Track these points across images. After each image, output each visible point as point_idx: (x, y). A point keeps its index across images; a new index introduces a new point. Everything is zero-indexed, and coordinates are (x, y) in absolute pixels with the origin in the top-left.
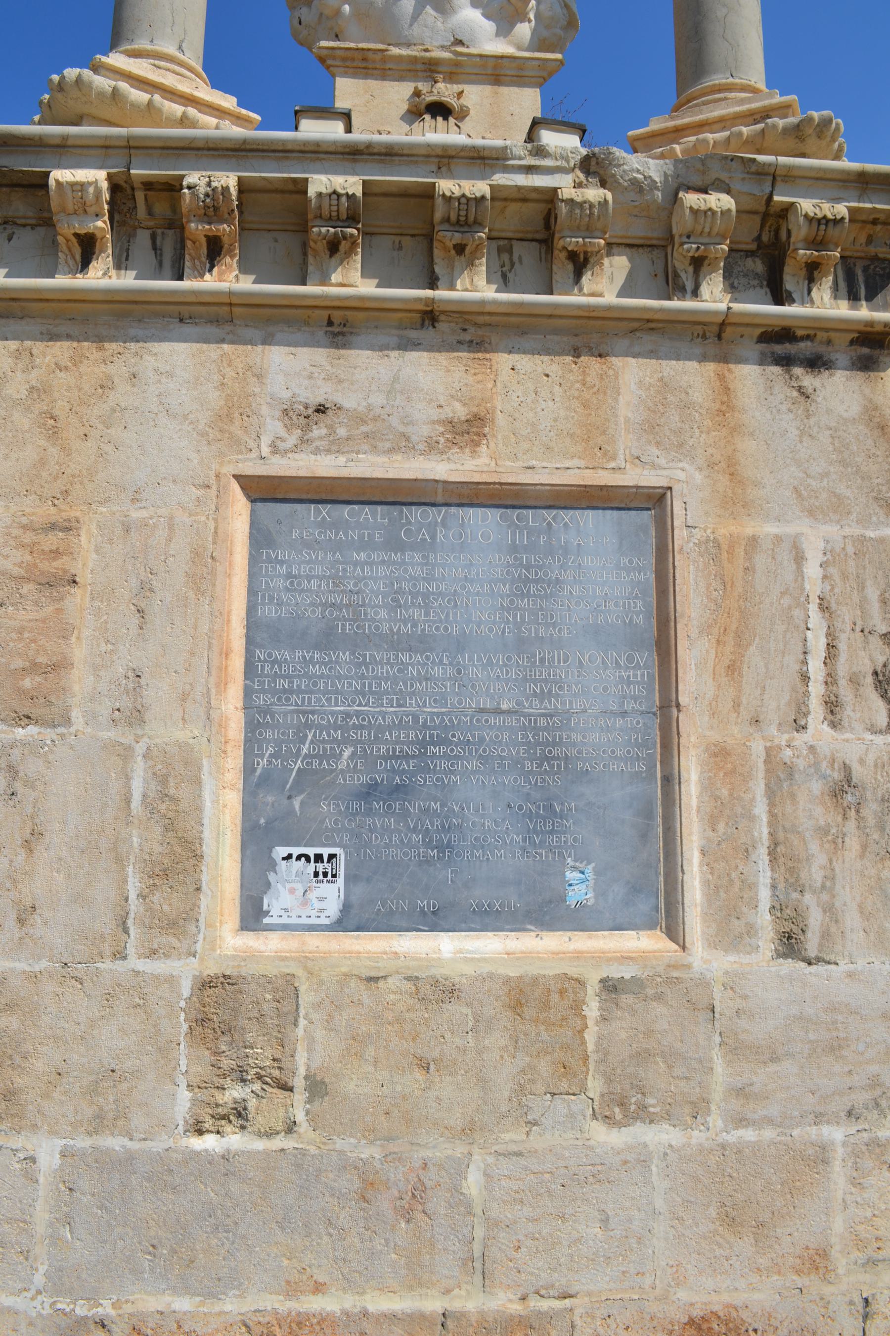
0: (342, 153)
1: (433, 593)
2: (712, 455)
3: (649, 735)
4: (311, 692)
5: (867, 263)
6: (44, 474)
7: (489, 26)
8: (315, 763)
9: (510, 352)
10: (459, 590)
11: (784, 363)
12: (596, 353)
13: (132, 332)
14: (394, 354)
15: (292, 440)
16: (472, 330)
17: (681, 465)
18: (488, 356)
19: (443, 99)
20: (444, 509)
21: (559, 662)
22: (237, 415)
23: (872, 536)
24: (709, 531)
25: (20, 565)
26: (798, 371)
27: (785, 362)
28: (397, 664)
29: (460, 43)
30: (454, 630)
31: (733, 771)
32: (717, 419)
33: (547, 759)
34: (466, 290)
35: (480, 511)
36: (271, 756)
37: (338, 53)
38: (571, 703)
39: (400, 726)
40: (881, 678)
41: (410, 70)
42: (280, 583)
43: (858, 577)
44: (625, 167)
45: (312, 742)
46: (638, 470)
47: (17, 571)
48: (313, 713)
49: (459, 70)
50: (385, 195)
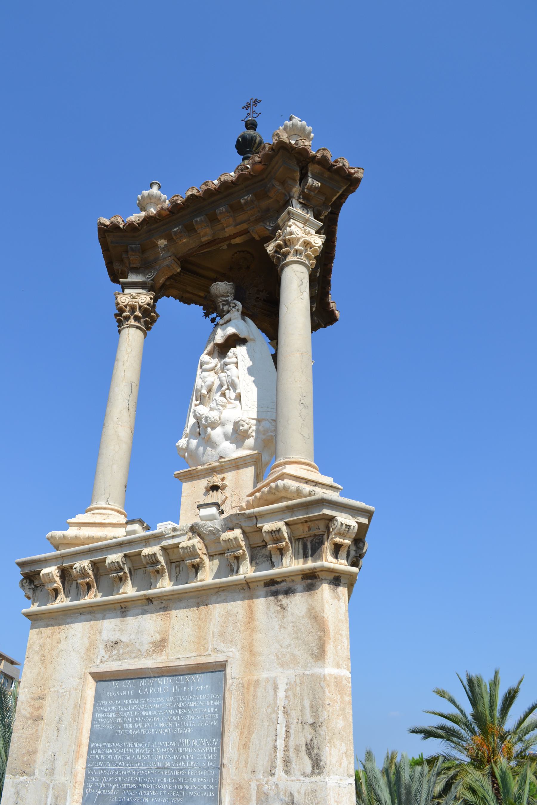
0: (118, 545)
1: (147, 716)
2: (244, 643)
3: (216, 778)
4: (105, 761)
5: (312, 538)
6: (39, 678)
7: (233, 446)
8: (104, 791)
9: (176, 609)
10: (155, 714)
11: (275, 594)
12: (205, 604)
13: (68, 620)
14: (140, 617)
15: (107, 657)
16: (164, 602)
17: (231, 650)
18: (168, 612)
19: (215, 484)
20: (153, 679)
21: (186, 745)
22: (92, 649)
23: (308, 673)
24: (240, 679)
25: (29, 713)
26: (280, 597)
27: (275, 594)
28: (133, 748)
29: (221, 457)
30: (152, 732)
31: (243, 797)
32: (247, 626)
33: (179, 790)
34: (160, 588)
35: (165, 678)
36: (92, 788)
37: (181, 474)
38: (189, 763)
39: (131, 775)
40: (309, 747)
41: (207, 473)
42: (101, 715)
43: (301, 695)
44: (205, 527)
45: (103, 783)
46: (216, 655)
47: (29, 716)
48: (105, 769)
49: (224, 468)
50: (136, 555)
